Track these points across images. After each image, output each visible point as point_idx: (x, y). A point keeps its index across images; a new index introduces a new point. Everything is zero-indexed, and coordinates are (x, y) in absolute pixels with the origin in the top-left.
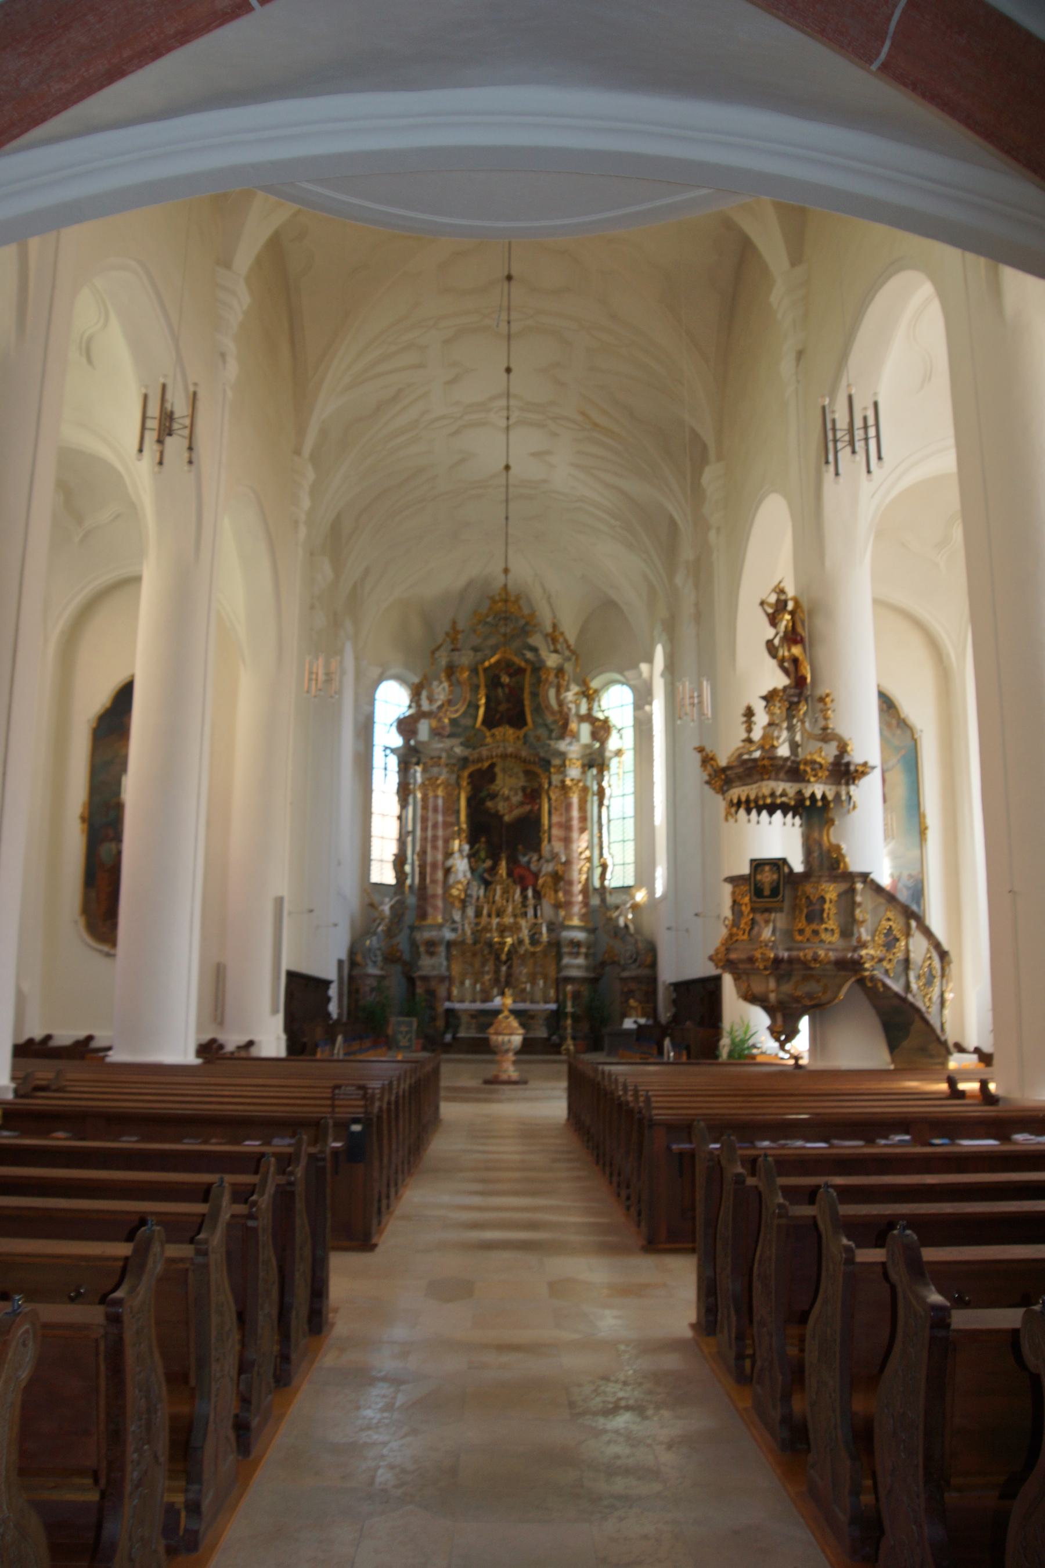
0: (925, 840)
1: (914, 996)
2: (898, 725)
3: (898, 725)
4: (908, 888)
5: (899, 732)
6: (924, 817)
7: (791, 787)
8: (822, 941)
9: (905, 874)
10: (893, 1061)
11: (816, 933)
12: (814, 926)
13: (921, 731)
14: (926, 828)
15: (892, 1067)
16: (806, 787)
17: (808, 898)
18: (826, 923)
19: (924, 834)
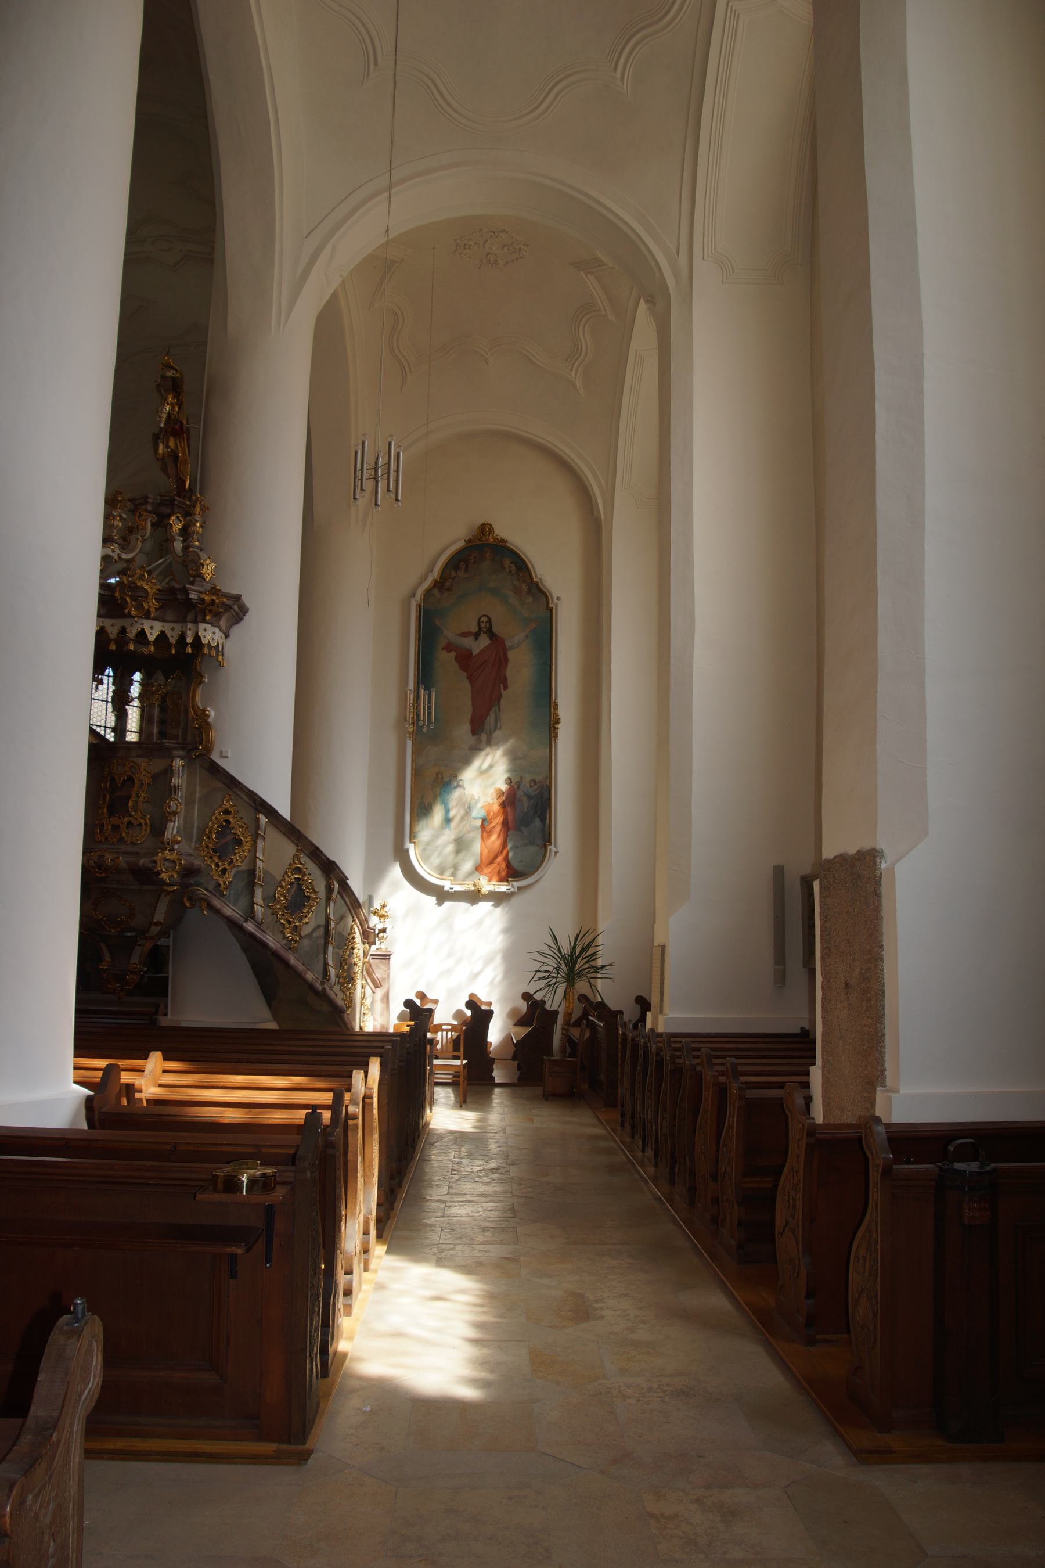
0: (556, 736)
1: (259, 925)
2: (529, 592)
3: (529, 592)
4: (529, 797)
5: (530, 599)
6: (556, 707)
7: (113, 625)
8: (121, 840)
9: (528, 778)
10: (275, 1018)
11: (116, 828)
12: (114, 820)
13: (558, 599)
14: (558, 721)
15: (273, 1026)
16: (132, 625)
17: (113, 779)
18: (131, 816)
19: (555, 728)
